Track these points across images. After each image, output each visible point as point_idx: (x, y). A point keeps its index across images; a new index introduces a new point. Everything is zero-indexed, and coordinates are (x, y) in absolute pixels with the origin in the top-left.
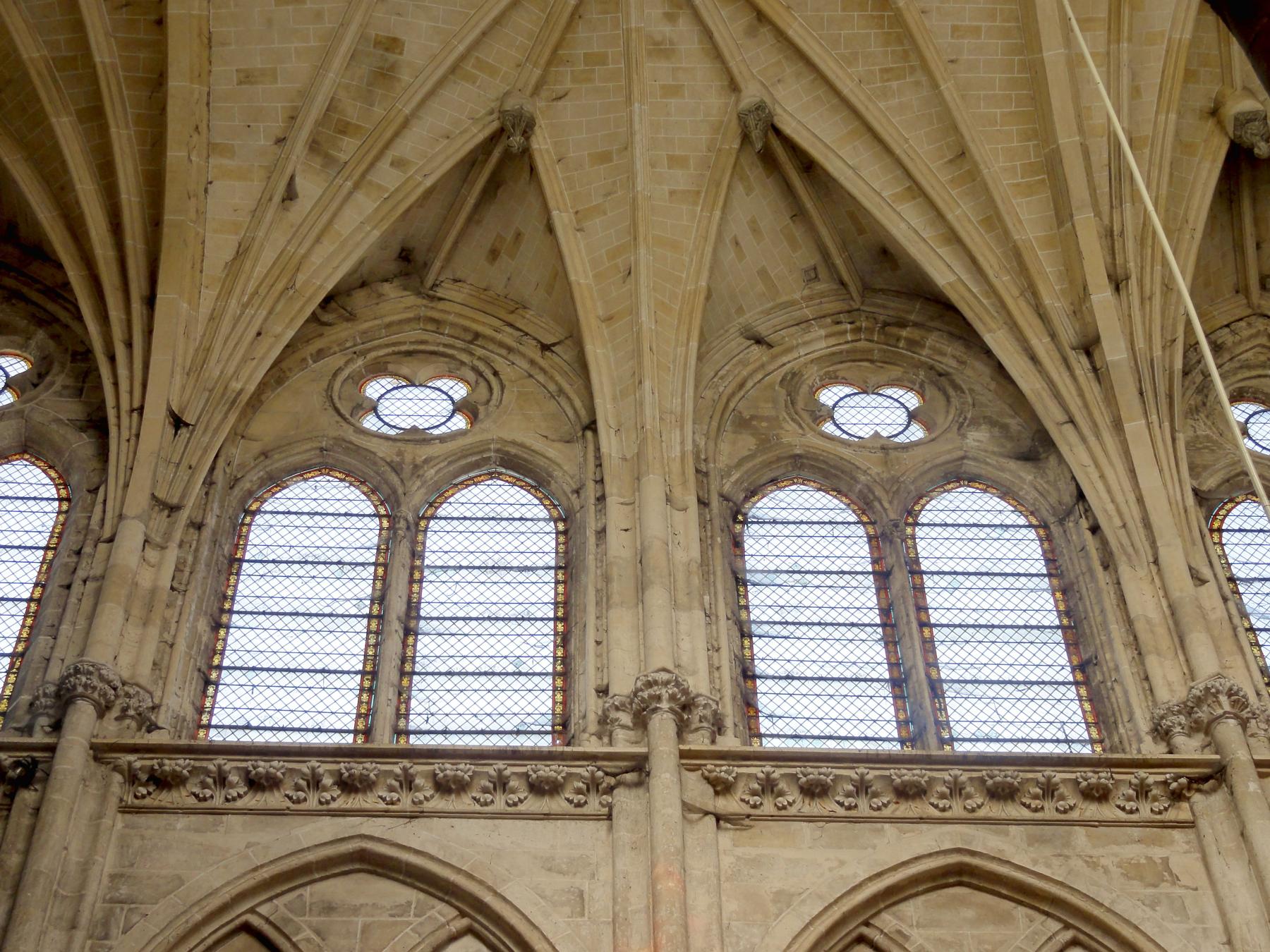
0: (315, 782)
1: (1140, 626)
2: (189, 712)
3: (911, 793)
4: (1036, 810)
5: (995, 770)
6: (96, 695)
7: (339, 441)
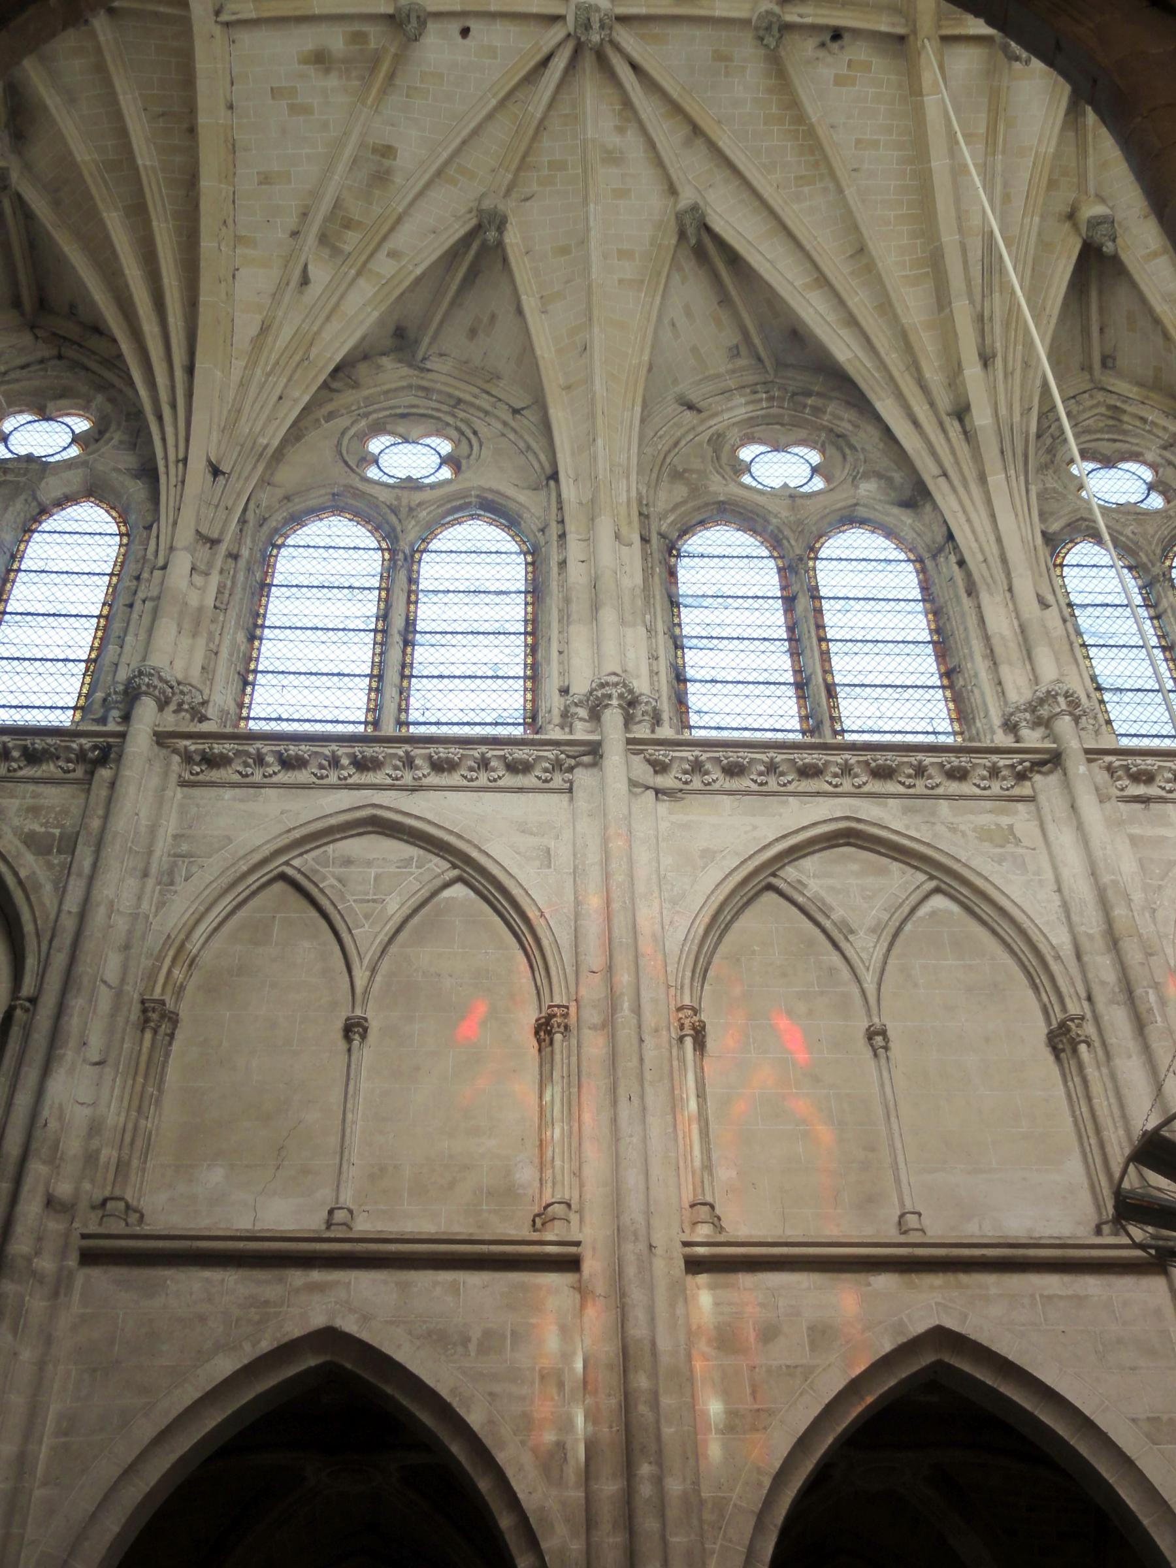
0: (335, 762)
1: (995, 641)
2: (232, 707)
4: (909, 787)
5: (878, 755)
6: (157, 692)
7: (349, 487)
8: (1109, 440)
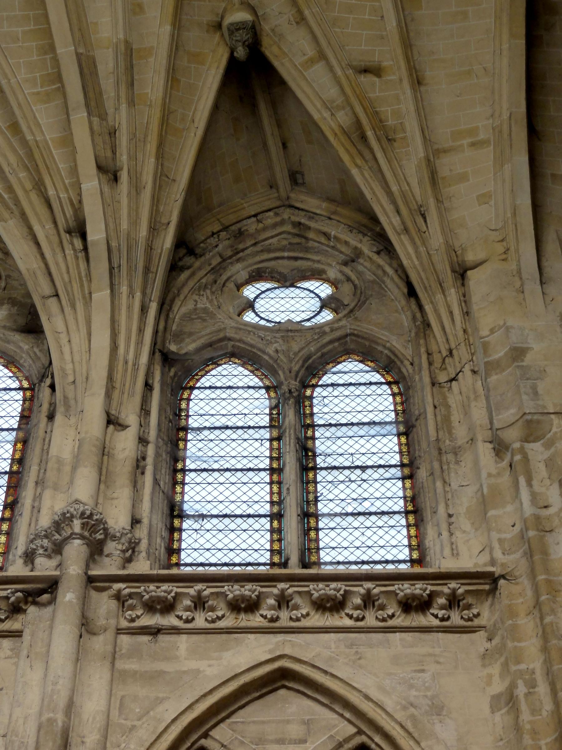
8: (289, 258)
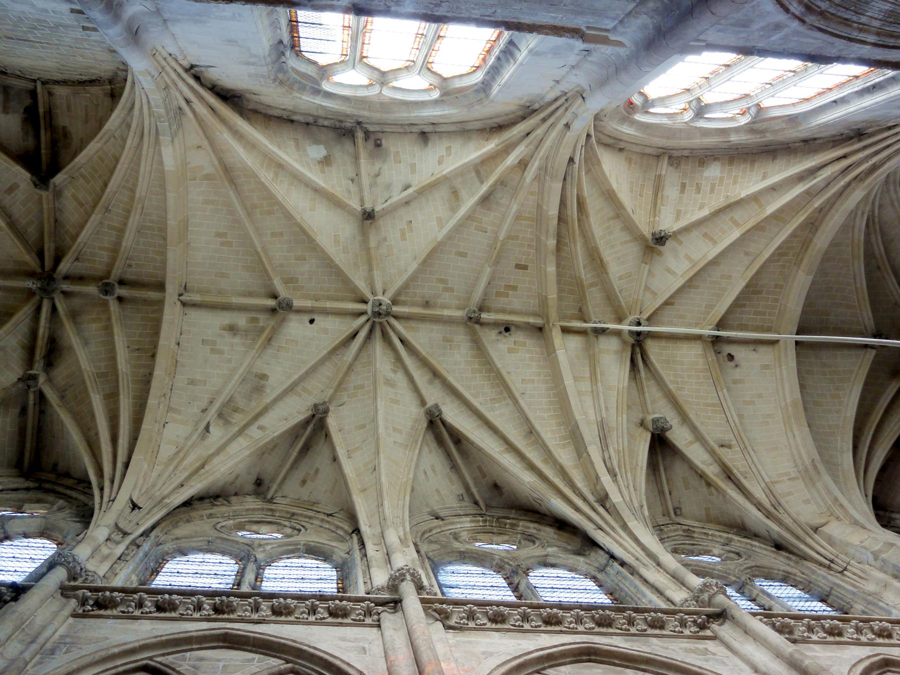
3: (553, 621)
8: (689, 544)
